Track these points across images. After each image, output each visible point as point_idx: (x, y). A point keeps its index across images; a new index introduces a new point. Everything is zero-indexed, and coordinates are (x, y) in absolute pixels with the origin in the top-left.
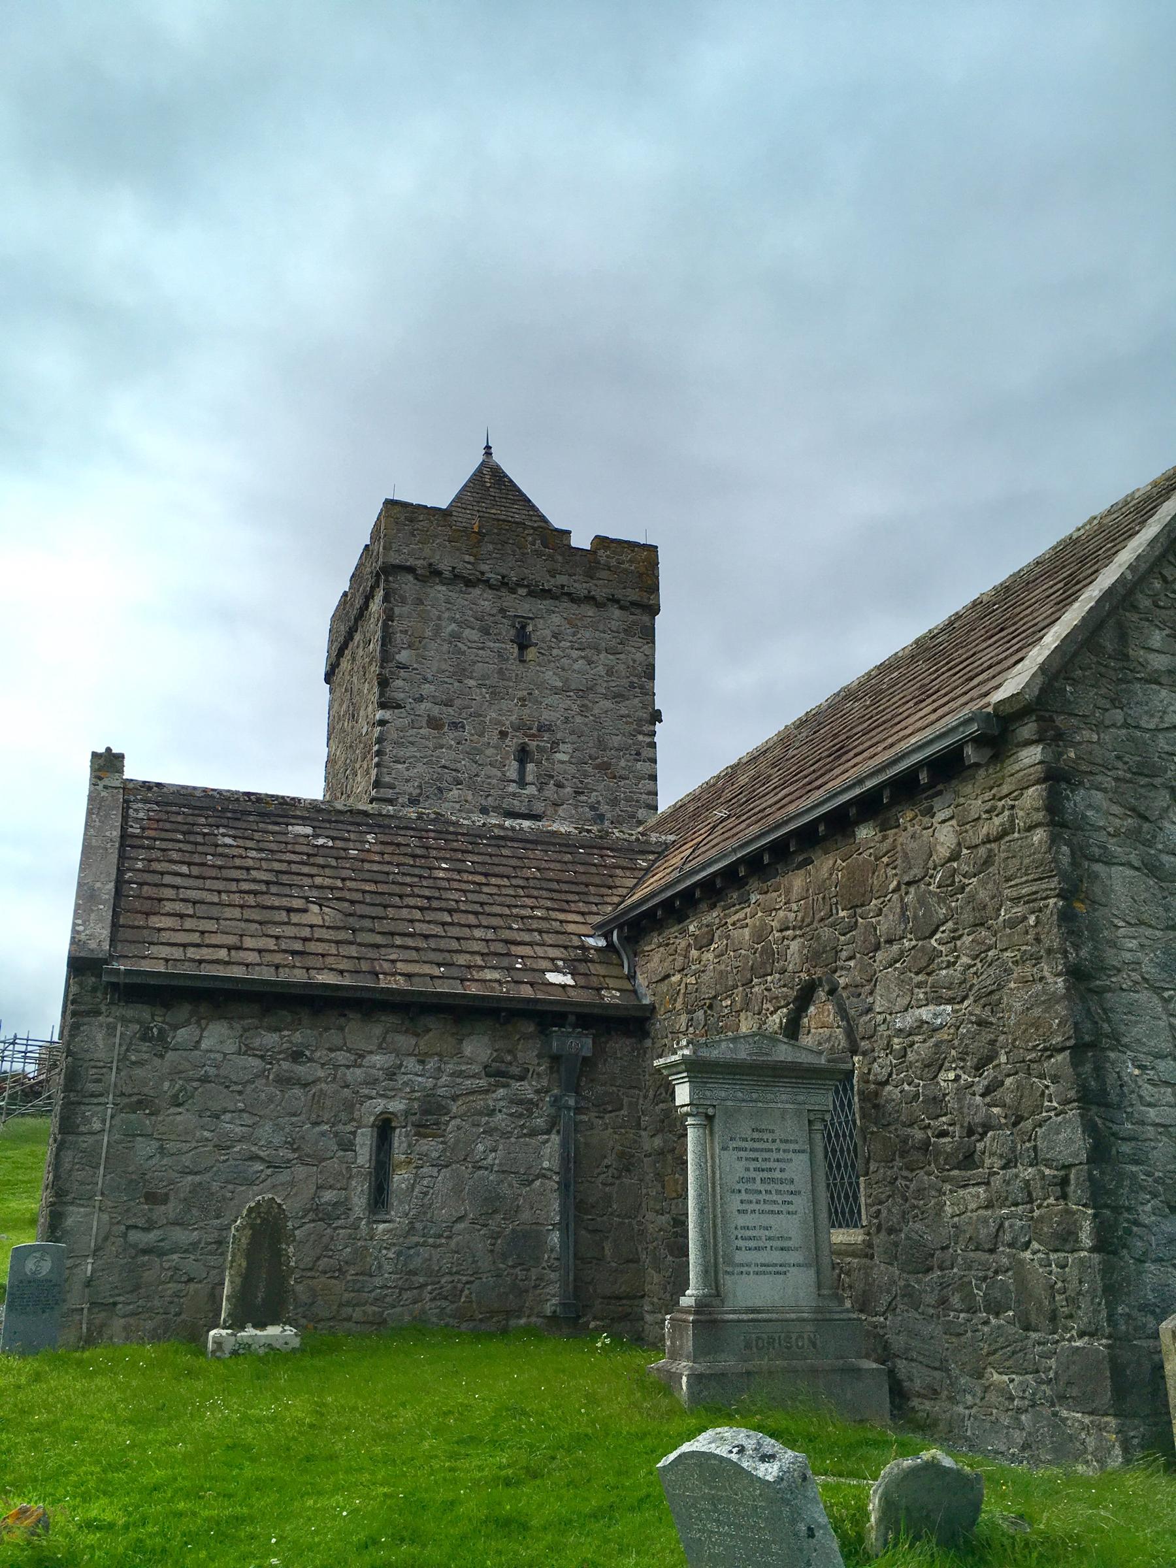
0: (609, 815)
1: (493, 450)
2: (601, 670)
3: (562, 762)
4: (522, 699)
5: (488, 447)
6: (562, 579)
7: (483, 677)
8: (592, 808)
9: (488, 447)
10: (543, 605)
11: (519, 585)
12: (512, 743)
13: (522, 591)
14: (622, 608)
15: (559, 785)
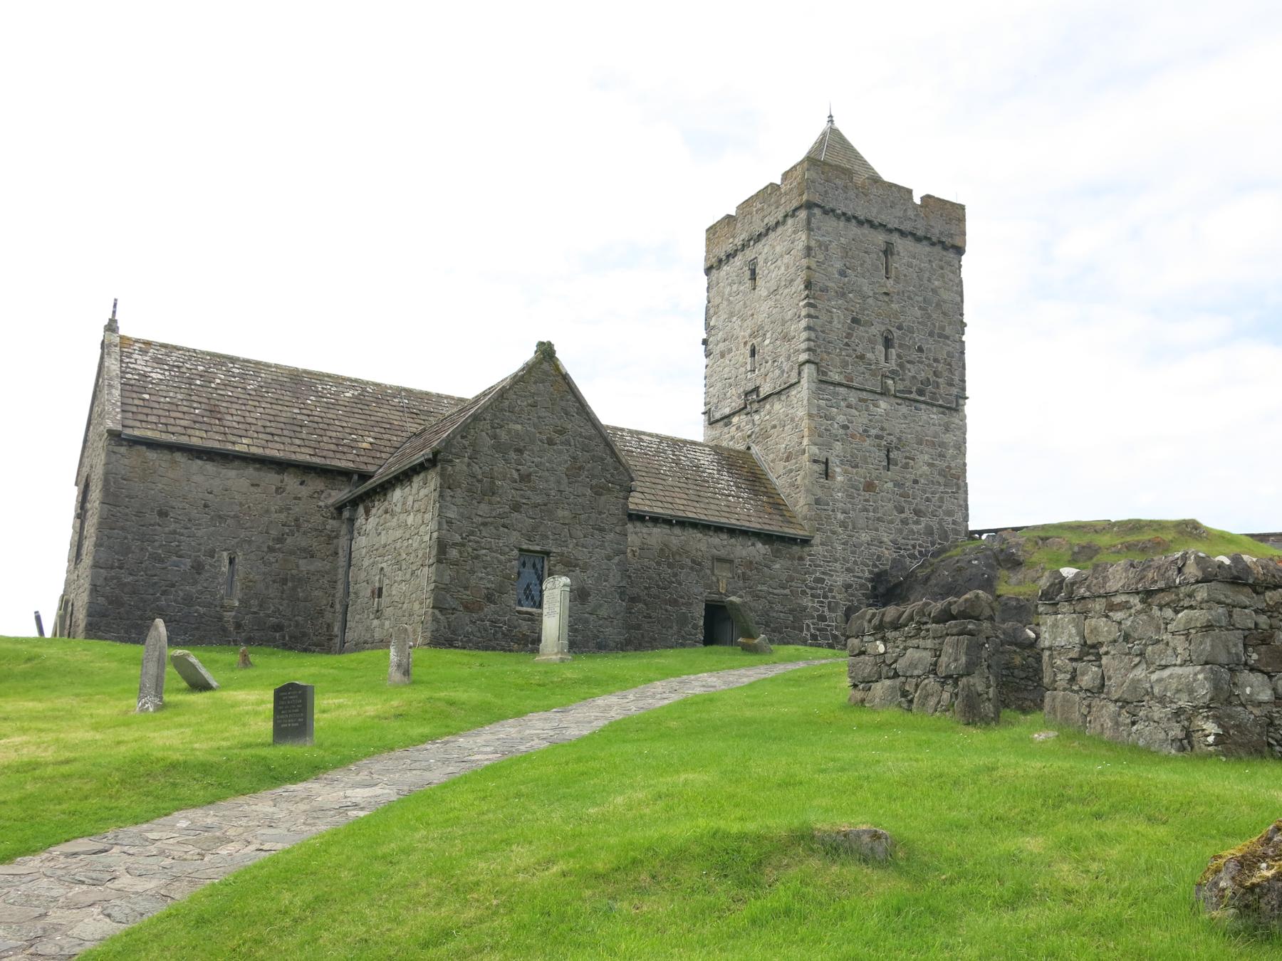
0: (786, 370)
1: (834, 119)
2: (783, 268)
3: (767, 346)
4: (753, 315)
5: (831, 116)
6: (766, 221)
7: (739, 312)
8: (780, 368)
9: (831, 116)
10: (760, 245)
11: (749, 241)
12: (748, 347)
13: (752, 243)
14: (793, 216)
15: (767, 362)
